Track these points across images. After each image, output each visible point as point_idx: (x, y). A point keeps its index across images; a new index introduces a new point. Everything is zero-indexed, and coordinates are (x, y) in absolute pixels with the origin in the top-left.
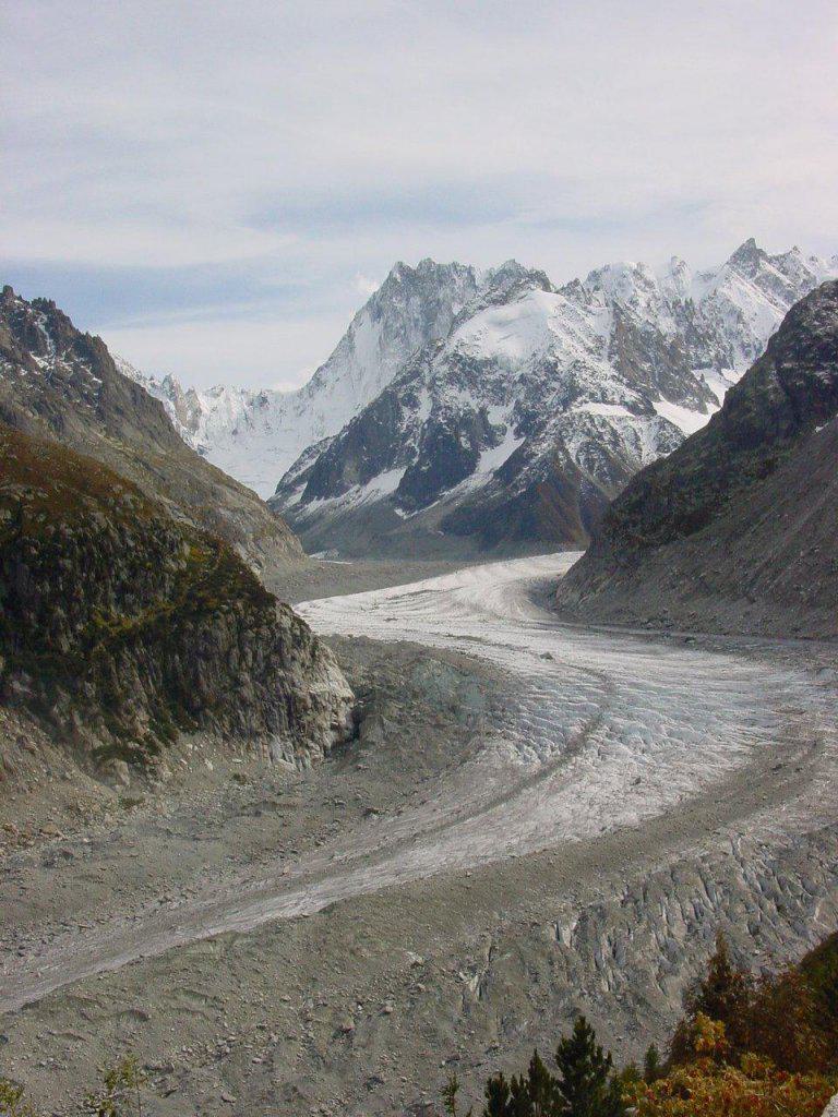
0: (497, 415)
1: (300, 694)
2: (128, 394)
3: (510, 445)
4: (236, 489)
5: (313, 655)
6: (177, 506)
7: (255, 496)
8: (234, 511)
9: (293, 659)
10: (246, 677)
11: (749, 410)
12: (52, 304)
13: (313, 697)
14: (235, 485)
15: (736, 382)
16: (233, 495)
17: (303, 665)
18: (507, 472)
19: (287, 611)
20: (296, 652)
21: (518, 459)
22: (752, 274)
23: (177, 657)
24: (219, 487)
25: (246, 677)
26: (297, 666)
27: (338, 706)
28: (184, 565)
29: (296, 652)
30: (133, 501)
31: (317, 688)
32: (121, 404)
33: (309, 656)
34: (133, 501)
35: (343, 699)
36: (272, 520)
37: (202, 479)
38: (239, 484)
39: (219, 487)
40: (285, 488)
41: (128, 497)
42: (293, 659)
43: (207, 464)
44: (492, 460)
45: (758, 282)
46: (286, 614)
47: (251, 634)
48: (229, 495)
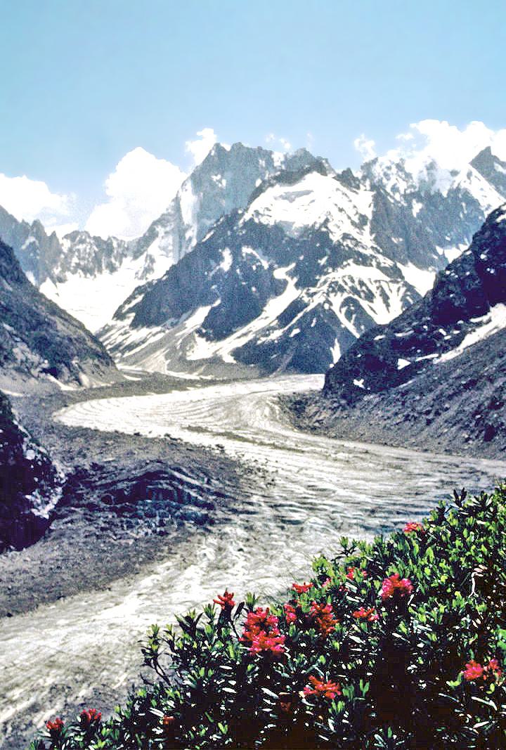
4: (66, 320)
6: (15, 332)
7: (81, 326)
11: (450, 292)
14: (67, 317)
16: (64, 325)
18: (285, 318)
21: (296, 306)
24: (53, 318)
37: (38, 311)
39: (53, 318)
43: (46, 299)
44: (275, 307)
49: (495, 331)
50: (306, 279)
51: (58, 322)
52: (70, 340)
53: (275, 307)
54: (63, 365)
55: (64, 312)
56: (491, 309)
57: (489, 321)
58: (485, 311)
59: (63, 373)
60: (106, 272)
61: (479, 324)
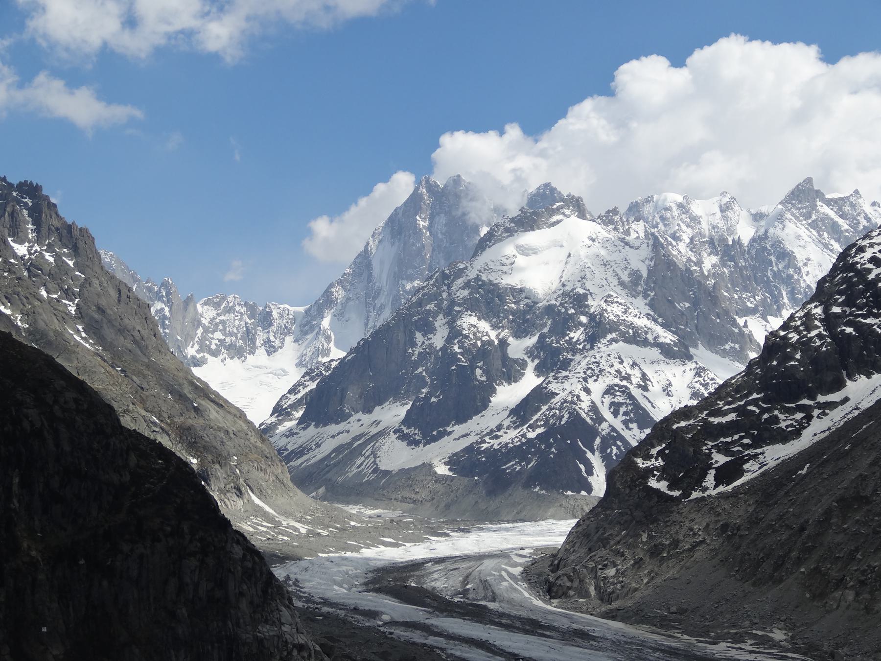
0: (518, 347)
1: (244, 636)
2: (114, 294)
3: (530, 381)
5: (265, 592)
8: (220, 429)
9: (241, 594)
10: (183, 612)
12: (38, 188)
13: (260, 642)
14: (221, 402)
15: (588, 105)
17: (251, 603)
18: (522, 412)
19: (241, 539)
20: (245, 587)
21: (539, 396)
22: (808, 216)
23: (105, 583)
25: (183, 612)
26: (244, 605)
27: (290, 653)
28: (127, 478)
29: (245, 587)
30: (76, 401)
31: (266, 631)
32: (103, 302)
33: (260, 593)
34: (76, 401)
35: (295, 646)
36: (259, 444)
38: (226, 401)
40: (279, 411)
41: (70, 395)
42: (241, 594)
44: (508, 395)
45: (814, 225)
46: (238, 543)
47: (193, 562)
48: (213, 413)
49: (856, 413)
50: (552, 361)
51: (212, 411)
52: (227, 432)
53: (508, 395)
54: (217, 466)
55: (217, 395)
56: (849, 383)
57: (846, 400)
58: (839, 385)
59: (217, 478)
60: (261, 352)
61: (832, 405)
